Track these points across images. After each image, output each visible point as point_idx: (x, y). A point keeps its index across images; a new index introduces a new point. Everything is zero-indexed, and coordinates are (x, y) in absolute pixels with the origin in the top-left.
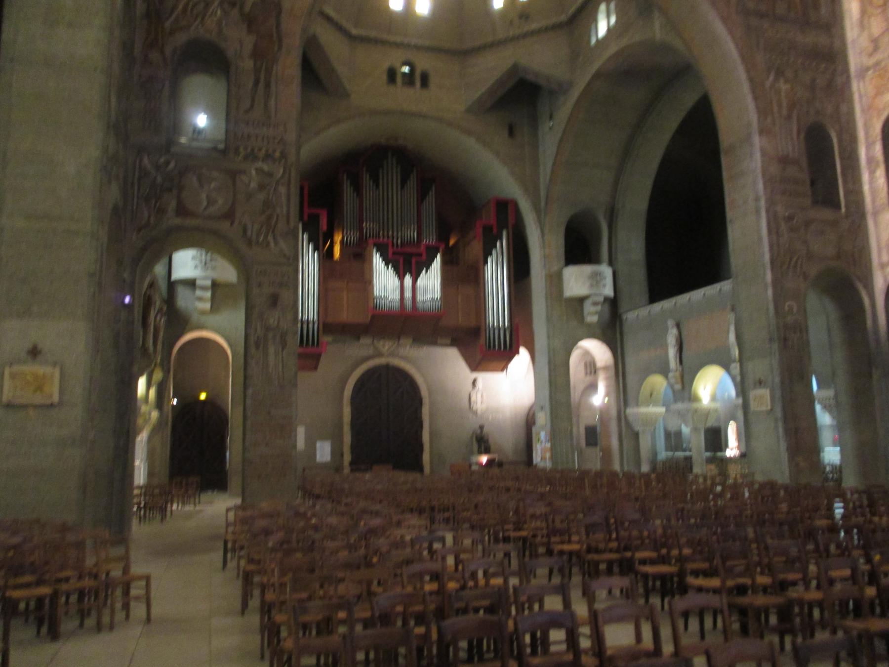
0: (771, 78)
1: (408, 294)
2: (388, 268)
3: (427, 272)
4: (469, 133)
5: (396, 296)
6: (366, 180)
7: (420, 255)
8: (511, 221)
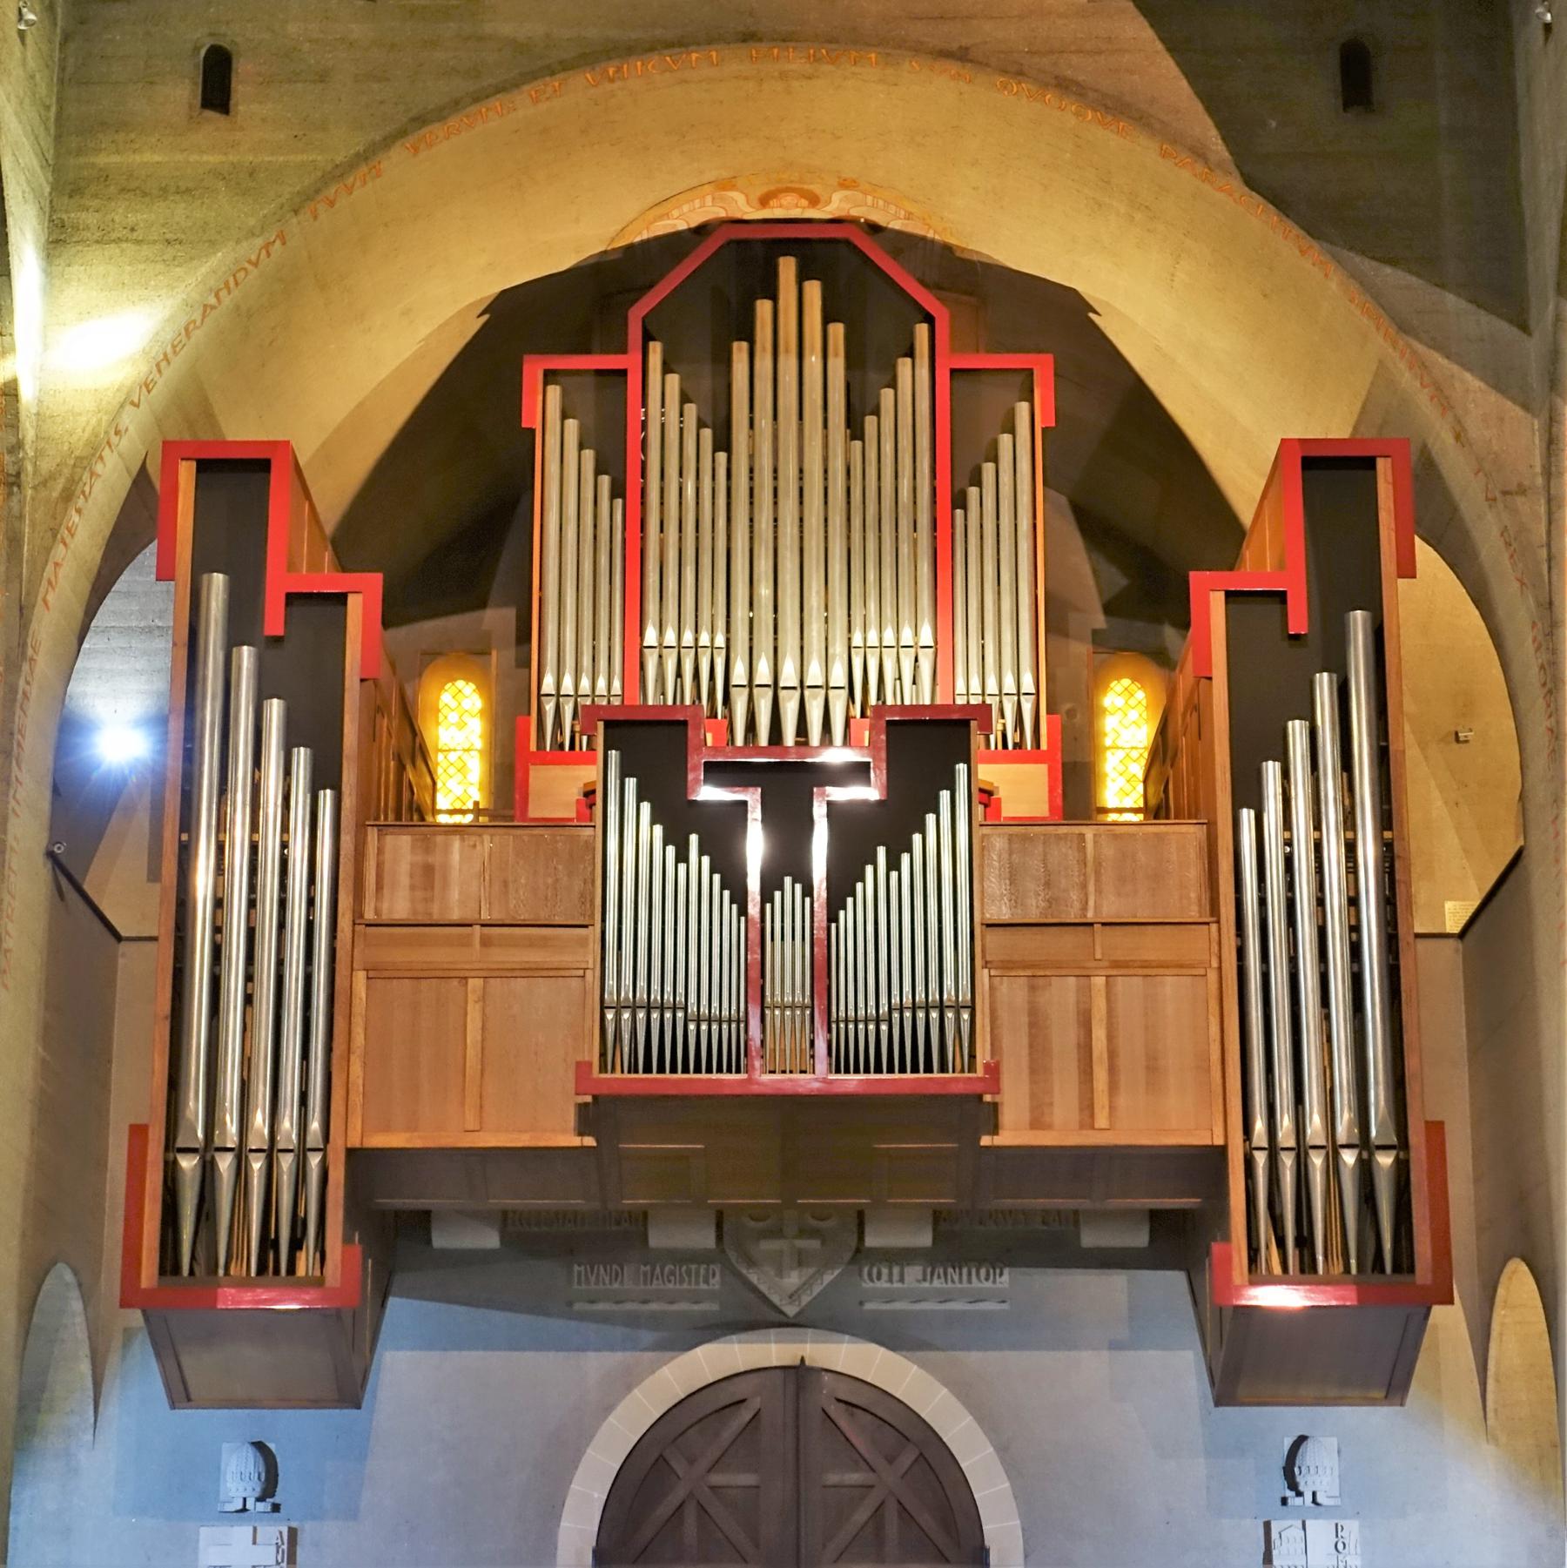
2: (682, 857)
3: (893, 864)
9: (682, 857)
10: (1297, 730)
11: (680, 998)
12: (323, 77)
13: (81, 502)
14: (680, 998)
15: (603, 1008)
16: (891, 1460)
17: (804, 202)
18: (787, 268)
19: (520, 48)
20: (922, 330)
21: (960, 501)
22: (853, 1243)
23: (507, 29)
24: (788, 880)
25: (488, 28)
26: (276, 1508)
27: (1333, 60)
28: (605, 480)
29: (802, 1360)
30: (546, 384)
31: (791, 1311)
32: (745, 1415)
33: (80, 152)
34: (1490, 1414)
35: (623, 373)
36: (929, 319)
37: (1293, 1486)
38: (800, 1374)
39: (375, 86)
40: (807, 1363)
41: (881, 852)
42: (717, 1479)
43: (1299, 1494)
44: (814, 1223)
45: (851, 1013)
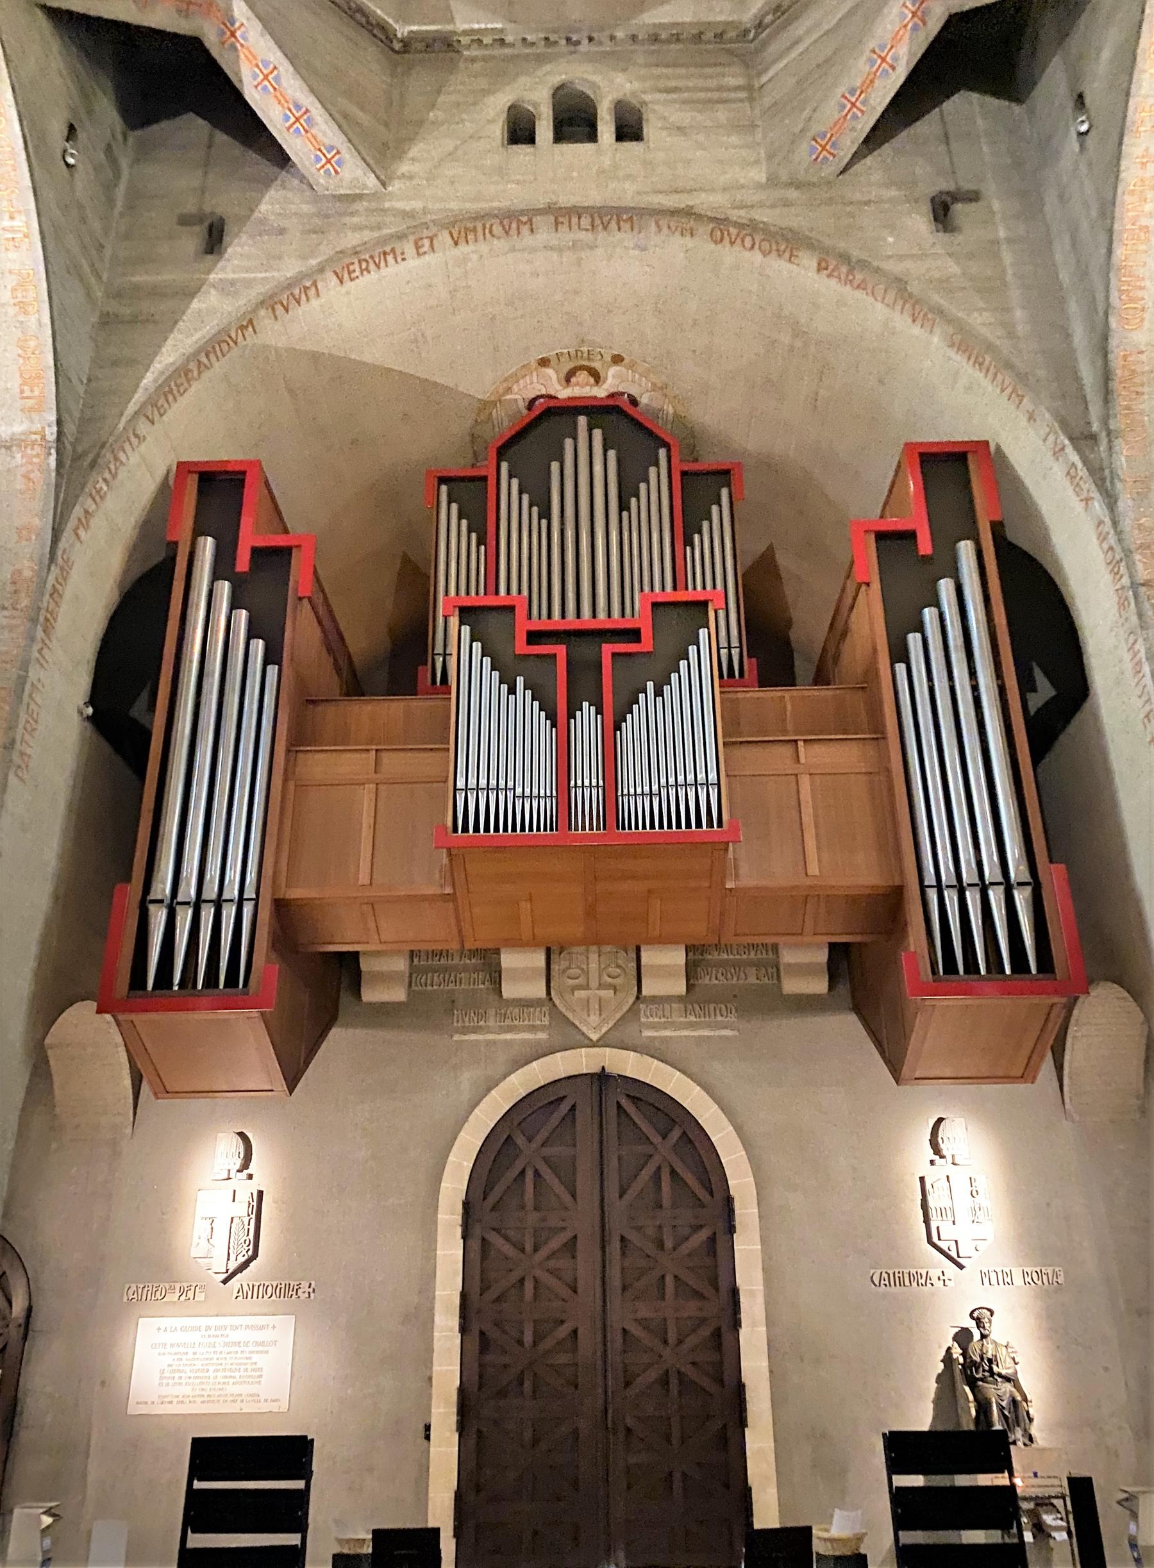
2: (512, 691)
3: (659, 692)
6: (509, 488)
9: (512, 691)
11: (510, 784)
12: (282, 231)
14: (510, 784)
15: (455, 789)
17: (592, 380)
18: (582, 420)
19: (406, 214)
20: (662, 453)
21: (689, 542)
23: (400, 205)
24: (585, 704)
25: (387, 205)
26: (250, 1177)
27: (926, 208)
28: (474, 536)
29: (603, 1068)
31: (595, 1037)
32: (564, 1107)
34: (1067, 1100)
35: (484, 479)
36: (667, 446)
37: (937, 1150)
38: (602, 1078)
39: (314, 236)
40: (607, 1071)
41: (650, 685)
42: (547, 1151)
43: (942, 1157)
44: (610, 980)
45: (632, 791)
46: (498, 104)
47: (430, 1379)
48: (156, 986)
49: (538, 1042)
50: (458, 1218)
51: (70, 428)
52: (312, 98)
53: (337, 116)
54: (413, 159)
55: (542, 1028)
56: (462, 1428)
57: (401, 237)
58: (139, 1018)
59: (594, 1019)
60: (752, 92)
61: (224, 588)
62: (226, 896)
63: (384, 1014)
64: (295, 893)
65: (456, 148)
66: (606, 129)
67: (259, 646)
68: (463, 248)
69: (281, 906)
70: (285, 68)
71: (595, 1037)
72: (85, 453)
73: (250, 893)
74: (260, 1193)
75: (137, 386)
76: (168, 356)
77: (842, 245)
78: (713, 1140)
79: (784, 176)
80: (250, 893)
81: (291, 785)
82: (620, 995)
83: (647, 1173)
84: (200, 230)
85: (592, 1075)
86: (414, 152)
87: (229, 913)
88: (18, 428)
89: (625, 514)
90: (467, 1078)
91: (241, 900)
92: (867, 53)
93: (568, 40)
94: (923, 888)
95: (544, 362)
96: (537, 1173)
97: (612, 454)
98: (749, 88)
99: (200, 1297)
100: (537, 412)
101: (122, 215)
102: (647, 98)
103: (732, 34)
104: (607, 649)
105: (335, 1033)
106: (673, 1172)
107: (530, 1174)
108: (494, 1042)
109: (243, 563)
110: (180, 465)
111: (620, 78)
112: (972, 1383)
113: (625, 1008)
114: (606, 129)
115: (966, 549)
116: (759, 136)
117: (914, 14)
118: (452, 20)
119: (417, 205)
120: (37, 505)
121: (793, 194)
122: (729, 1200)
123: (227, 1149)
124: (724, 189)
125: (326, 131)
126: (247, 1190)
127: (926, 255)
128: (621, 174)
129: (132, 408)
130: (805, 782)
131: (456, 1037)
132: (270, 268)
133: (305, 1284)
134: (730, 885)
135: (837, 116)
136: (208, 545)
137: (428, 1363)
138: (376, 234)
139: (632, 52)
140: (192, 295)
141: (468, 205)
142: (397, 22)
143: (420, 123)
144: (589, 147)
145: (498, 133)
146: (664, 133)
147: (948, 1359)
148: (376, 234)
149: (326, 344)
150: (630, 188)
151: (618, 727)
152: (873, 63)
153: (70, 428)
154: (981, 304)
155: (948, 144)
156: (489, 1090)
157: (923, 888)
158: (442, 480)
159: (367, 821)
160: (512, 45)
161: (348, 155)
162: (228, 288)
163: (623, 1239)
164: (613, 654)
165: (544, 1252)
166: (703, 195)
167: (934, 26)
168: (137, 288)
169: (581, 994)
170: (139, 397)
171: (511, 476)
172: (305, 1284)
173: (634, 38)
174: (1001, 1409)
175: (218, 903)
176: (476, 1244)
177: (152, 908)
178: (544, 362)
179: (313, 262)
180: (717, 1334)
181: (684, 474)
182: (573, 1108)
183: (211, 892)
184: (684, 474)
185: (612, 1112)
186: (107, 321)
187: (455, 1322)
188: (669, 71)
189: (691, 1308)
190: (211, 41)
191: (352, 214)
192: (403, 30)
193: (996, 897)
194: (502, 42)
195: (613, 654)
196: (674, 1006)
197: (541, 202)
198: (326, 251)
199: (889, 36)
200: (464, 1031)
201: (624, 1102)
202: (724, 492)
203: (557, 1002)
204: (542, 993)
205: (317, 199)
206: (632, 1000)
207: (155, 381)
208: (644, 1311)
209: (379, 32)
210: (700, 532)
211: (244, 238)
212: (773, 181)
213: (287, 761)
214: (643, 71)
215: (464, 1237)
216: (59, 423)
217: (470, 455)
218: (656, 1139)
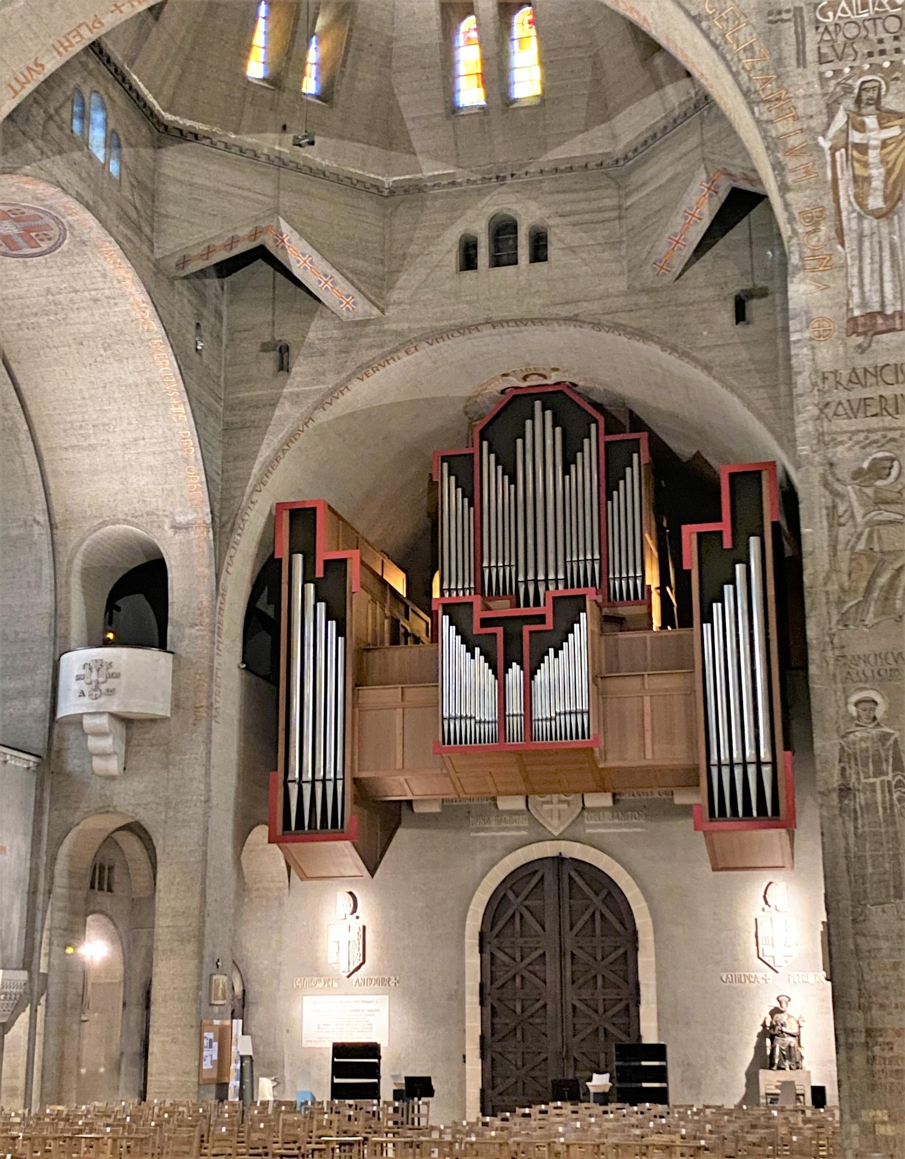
0: (840, 119)
1: (515, 706)
2: (473, 657)
3: (556, 655)
4: (642, 334)
5: (487, 711)
7: (541, 619)
8: (771, 511)
9: (473, 657)
10: (728, 589)
12: (323, 354)
13: (240, 531)
16: (597, 895)
18: (538, 404)
19: (398, 334)
20: (593, 426)
21: (609, 497)
22: (581, 805)
23: (393, 327)
24: (514, 664)
25: (386, 327)
27: (731, 305)
28: (466, 500)
30: (443, 461)
33: (233, 393)
35: (472, 455)
37: (766, 903)
38: (559, 860)
41: (551, 651)
42: (527, 903)
46: (451, 239)
47: (464, 1031)
48: (296, 828)
49: (522, 836)
50: (477, 941)
51: (217, 507)
52: (334, 270)
53: (350, 275)
54: (400, 288)
55: (524, 828)
56: (483, 1056)
57: (397, 350)
58: (288, 845)
59: (555, 822)
60: (621, 212)
61: (311, 587)
62: (327, 777)
63: (427, 820)
64: (363, 775)
65: (428, 275)
66: (524, 253)
67: (332, 624)
68: (436, 345)
69: (355, 780)
70: (316, 257)
71: (556, 834)
72: (227, 522)
73: (339, 776)
74: (364, 927)
75: (250, 474)
76: (265, 453)
77: (673, 340)
78: (627, 895)
79: (637, 284)
80: (339, 776)
81: (357, 710)
82: (572, 807)
83: (586, 916)
84: (274, 354)
85: (553, 858)
86: (401, 282)
87: (330, 786)
88: (190, 517)
89: (567, 477)
90: (481, 858)
91: (336, 779)
92: (681, 213)
93: (498, 177)
94: (709, 766)
95: (505, 375)
96: (522, 916)
97: (558, 430)
98: (620, 207)
99: (336, 985)
100: (508, 398)
101: (227, 347)
102: (551, 222)
103: (609, 161)
104: (526, 629)
105: (400, 831)
106: (602, 915)
107: (517, 917)
108: (493, 837)
109: (320, 573)
110: (278, 504)
111: (533, 206)
112: (772, 1038)
113: (575, 815)
114: (524, 253)
115: (754, 542)
116: (623, 253)
117: (709, 189)
118: (421, 171)
119: (405, 325)
120: (206, 561)
121: (644, 299)
122: (635, 932)
123: (343, 902)
124: (599, 299)
125: (345, 287)
126: (357, 926)
127: (728, 345)
128: (533, 290)
129: (248, 490)
130: (647, 699)
131: (472, 834)
132: (319, 382)
133: (393, 978)
134: (601, 766)
135: (667, 249)
136: (299, 559)
137: (463, 1021)
138: (380, 351)
139: (541, 181)
140: (274, 405)
141: (436, 324)
142: (383, 176)
143: (404, 256)
144: (511, 269)
145: (454, 261)
146: (560, 253)
147: (764, 1025)
148: (380, 351)
149: (359, 406)
150: (538, 301)
151: (532, 678)
152: (686, 218)
153: (217, 507)
154: (759, 383)
155: (751, 247)
156: (493, 866)
157: (709, 766)
158: (444, 459)
159: (399, 731)
160: (461, 184)
161: (360, 299)
162: (296, 399)
163: (573, 954)
164: (531, 632)
165: (527, 961)
166: (585, 304)
167: (723, 195)
168: (242, 402)
169: (546, 807)
170: (252, 481)
171: (490, 452)
172: (393, 978)
173: (542, 172)
174: (781, 1050)
175: (324, 781)
176: (487, 957)
177: (290, 785)
178: (505, 375)
179: (344, 375)
180: (627, 1008)
181: (607, 443)
182: (543, 877)
183: (320, 775)
184: (607, 443)
185: (566, 880)
186: (228, 428)
187: (477, 999)
188: (567, 196)
189: (612, 994)
190: (271, 247)
191: (366, 336)
192: (388, 181)
193: (752, 770)
194: (453, 183)
195: (531, 632)
196: (608, 813)
197: (482, 316)
198: (351, 366)
199: (694, 203)
200: (478, 830)
201: (573, 874)
202: (635, 456)
203: (533, 812)
204: (523, 807)
205: (343, 325)
206: (579, 810)
207: (260, 470)
208: (586, 994)
209: (374, 189)
210: (618, 490)
211: (301, 358)
212: (631, 290)
213: (353, 694)
214: (550, 198)
215: (481, 951)
216: (212, 512)
217: (467, 420)
218: (591, 895)
